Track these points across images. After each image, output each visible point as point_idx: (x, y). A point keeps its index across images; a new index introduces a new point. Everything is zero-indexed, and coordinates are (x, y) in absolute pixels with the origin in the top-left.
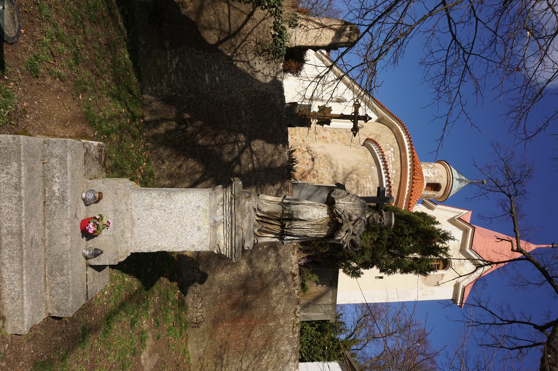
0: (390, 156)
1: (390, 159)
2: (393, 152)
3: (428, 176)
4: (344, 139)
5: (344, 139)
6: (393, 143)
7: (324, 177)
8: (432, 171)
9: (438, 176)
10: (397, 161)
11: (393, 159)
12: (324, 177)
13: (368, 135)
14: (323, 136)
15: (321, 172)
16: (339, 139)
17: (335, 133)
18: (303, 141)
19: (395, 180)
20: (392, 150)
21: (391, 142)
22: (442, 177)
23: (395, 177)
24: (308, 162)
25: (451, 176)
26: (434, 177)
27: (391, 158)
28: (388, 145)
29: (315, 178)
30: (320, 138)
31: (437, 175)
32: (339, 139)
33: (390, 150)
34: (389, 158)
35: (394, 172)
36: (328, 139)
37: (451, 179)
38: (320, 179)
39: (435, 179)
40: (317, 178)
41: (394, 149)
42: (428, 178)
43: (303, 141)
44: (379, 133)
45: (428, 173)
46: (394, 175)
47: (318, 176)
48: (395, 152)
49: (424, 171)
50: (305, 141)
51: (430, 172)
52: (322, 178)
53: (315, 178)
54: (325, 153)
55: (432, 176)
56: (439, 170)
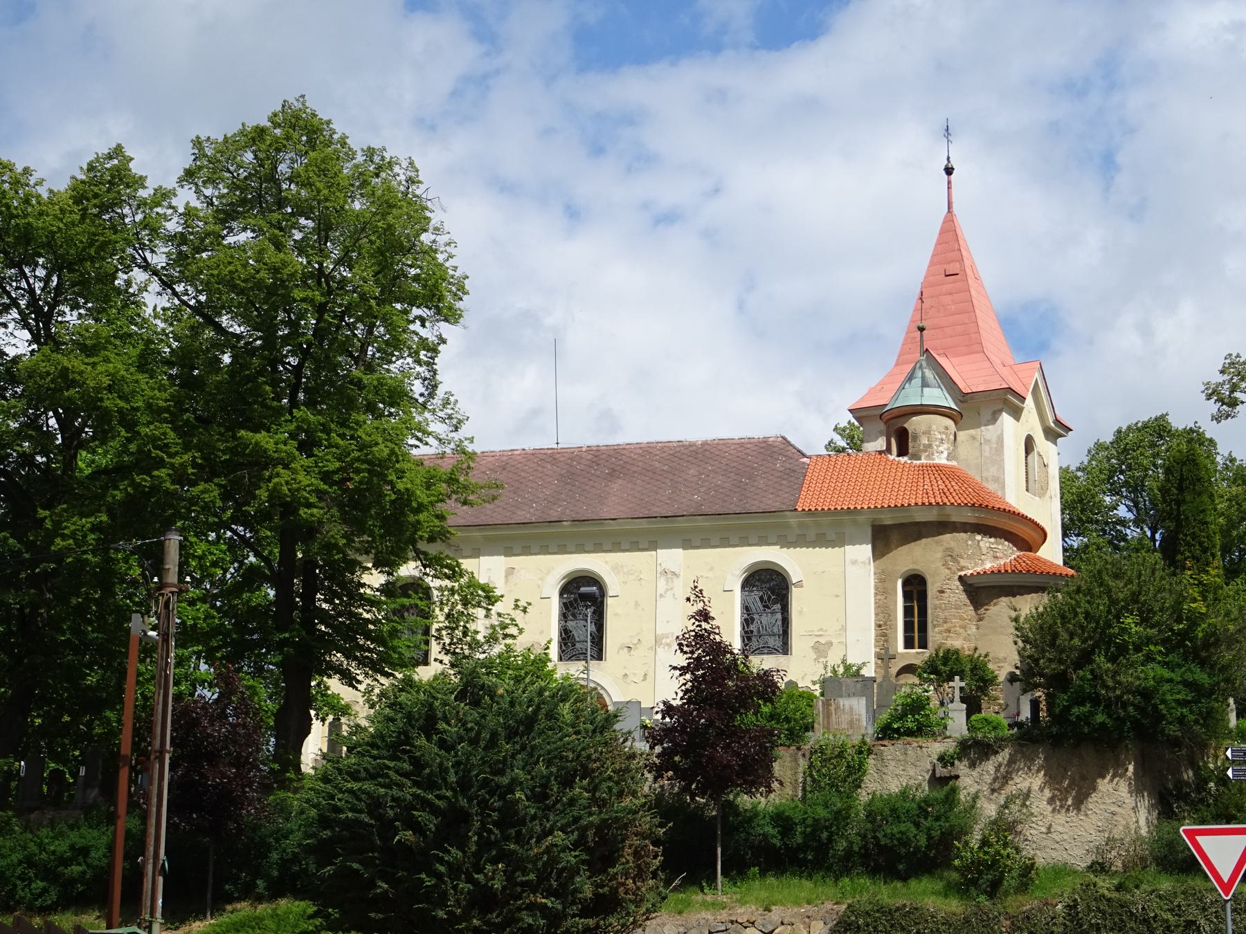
0: (987, 545)
3: (945, 454)
4: (962, 619)
5: (962, 619)
13: (948, 572)
16: (964, 627)
17: (949, 631)
22: (947, 428)
28: (970, 543)
31: (944, 436)
33: (979, 541)
44: (941, 549)
49: (937, 461)
51: (941, 449)
55: (945, 446)
56: (934, 427)
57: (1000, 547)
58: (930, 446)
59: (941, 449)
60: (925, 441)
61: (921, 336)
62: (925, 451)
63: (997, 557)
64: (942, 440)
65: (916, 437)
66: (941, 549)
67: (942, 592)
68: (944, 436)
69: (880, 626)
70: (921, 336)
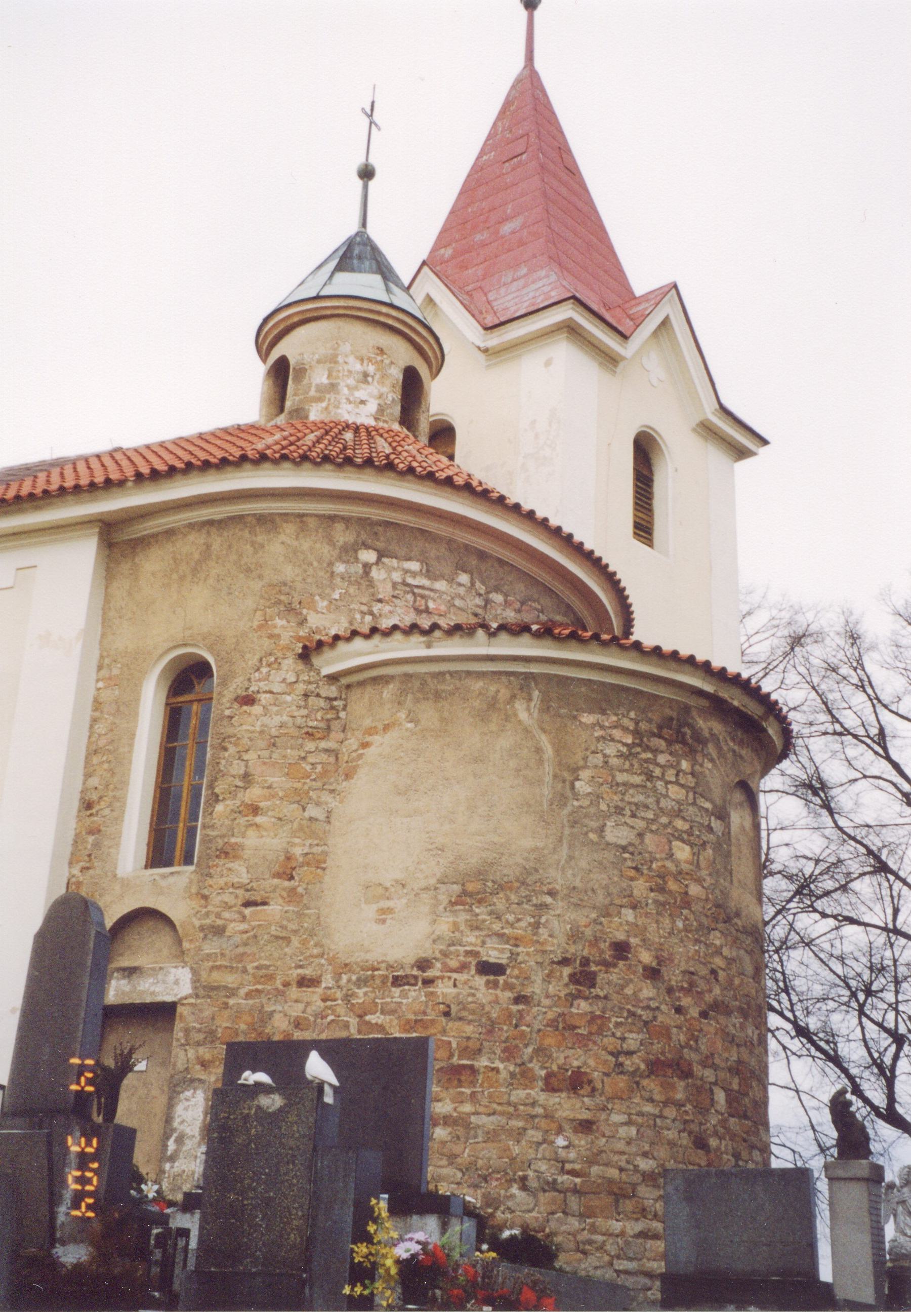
0: (397, 576)
1: (410, 580)
2: (381, 555)
6: (331, 542)
7: (588, 932)
8: (351, 381)
9: (379, 365)
10: (423, 552)
11: (414, 566)
12: (588, 932)
14: (278, 875)
15: (562, 939)
18: (304, 982)
19: (493, 582)
20: (368, 556)
21: (326, 551)
22: (381, 351)
23: (483, 583)
24: (509, 994)
25: (384, 309)
26: (381, 382)
27: (407, 571)
28: (340, 568)
29: (594, 974)
30: (293, 890)
32: (301, 799)
33: (367, 567)
34: (405, 584)
35: (464, 578)
36: (298, 851)
37: (394, 313)
38: (602, 952)
39: (388, 382)
40: (594, 968)
41: (367, 547)
42: (381, 410)
43: (304, 982)
45: (363, 402)
46: (478, 584)
47: (586, 962)
48: (380, 545)
50: (308, 972)
51: (361, 394)
52: (595, 942)
53: (594, 974)
54: (444, 899)
57: (441, 585)
58: (333, 387)
59: (361, 394)
60: (319, 377)
61: (366, 188)
62: (320, 400)
63: (427, 611)
64: (366, 375)
65: (301, 372)
66: (257, 585)
67: (249, 700)
68: (371, 369)
69: (88, 805)
70: (366, 188)
